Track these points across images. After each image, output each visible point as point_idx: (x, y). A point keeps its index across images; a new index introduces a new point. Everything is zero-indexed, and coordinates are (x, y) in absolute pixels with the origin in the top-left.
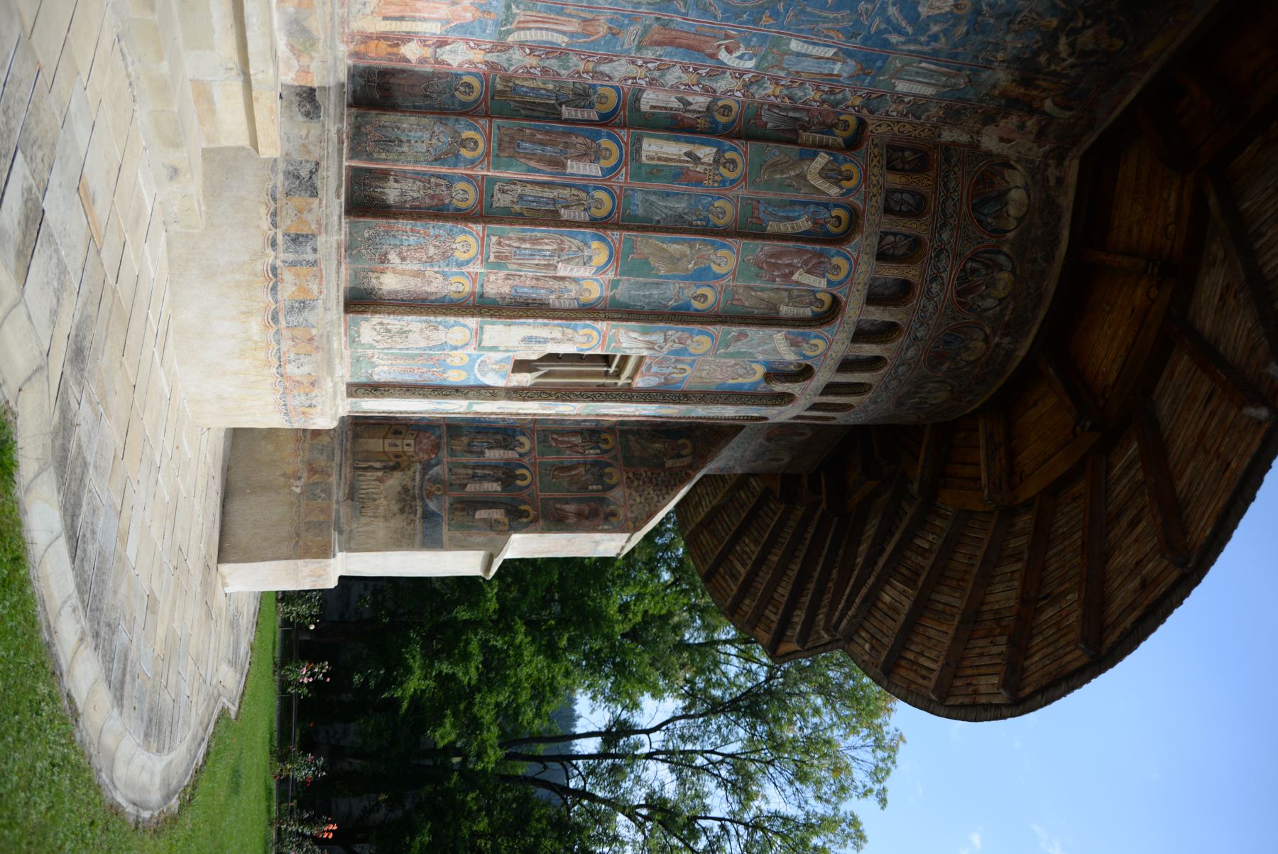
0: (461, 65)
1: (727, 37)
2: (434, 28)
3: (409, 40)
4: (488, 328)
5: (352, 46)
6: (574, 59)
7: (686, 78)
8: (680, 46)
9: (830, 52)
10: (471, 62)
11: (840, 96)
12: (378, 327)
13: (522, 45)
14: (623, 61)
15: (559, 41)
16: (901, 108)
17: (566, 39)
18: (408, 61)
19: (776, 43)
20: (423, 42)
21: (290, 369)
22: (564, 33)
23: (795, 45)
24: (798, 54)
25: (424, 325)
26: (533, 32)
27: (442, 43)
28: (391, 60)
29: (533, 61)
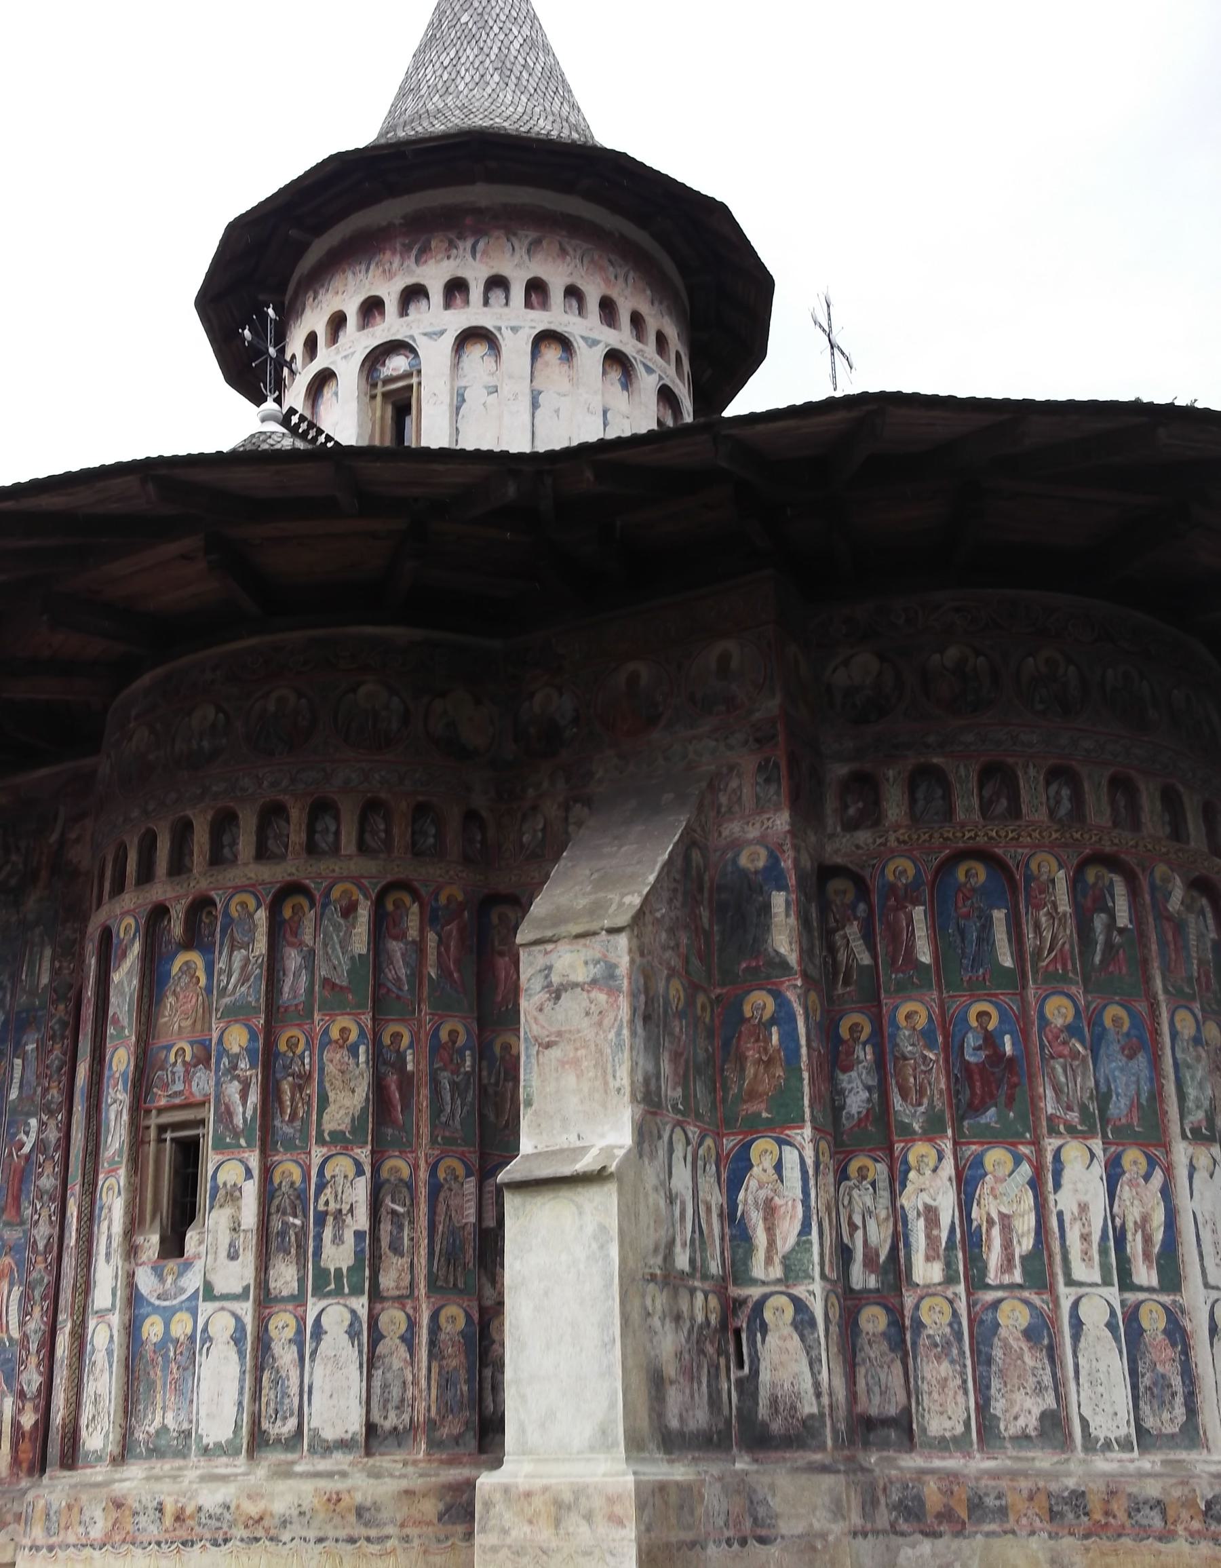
0: (41, 1374)
1: (10, 1154)
2: (8, 1403)
3: (19, 1422)
4: (95, 1308)
5: (21, 1475)
6: (35, 1275)
7: (48, 1170)
8: (20, 1190)
9: (18, 1062)
10: (38, 1365)
11: (57, 1027)
12: (90, 1429)
13: (22, 1324)
14: (34, 1232)
15: (19, 1294)
16: (65, 964)
17: (16, 1288)
18: (36, 1422)
19: (14, 1111)
20: (20, 1411)
21: (96, 1533)
22: (10, 1292)
23: (14, 1095)
24: (21, 1087)
25: (91, 1377)
26: (10, 1318)
27: (22, 1395)
28: (36, 1439)
29: (37, 1310)
